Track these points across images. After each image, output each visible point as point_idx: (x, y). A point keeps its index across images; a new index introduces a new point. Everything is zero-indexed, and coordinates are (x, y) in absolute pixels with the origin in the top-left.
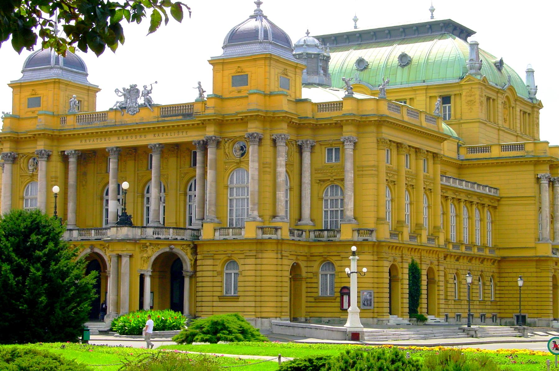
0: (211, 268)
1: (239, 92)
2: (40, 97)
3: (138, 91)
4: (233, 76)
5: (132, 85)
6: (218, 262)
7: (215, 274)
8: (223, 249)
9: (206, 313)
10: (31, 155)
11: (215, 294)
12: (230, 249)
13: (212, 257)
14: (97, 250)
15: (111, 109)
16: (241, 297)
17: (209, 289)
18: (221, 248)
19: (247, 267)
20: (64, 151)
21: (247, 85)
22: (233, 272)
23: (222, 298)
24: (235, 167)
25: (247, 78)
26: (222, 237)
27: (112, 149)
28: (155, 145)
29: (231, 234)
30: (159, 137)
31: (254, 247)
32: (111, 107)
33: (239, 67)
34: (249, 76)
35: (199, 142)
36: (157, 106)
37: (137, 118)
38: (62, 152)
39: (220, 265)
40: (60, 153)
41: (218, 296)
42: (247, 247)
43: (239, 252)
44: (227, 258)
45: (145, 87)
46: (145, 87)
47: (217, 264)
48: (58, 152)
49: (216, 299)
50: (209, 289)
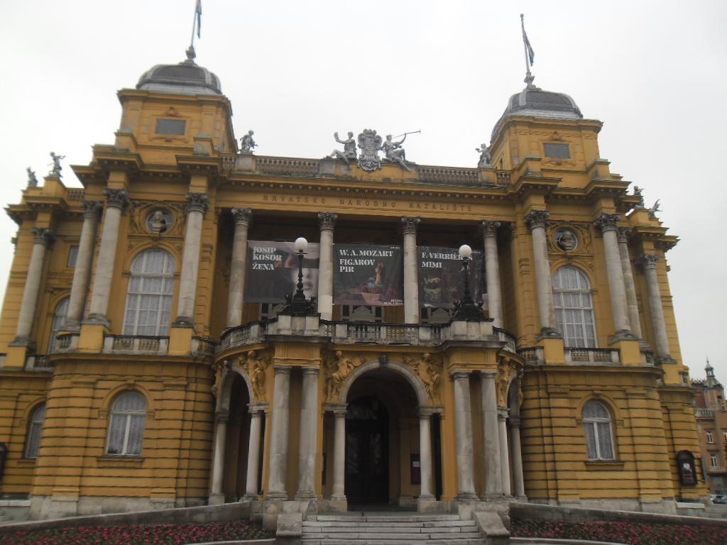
0: (566, 412)
1: (559, 164)
2: (184, 121)
3: (378, 140)
4: (544, 144)
5: (368, 129)
6: (577, 404)
7: (573, 422)
8: (583, 382)
9: (567, 492)
10: (158, 205)
11: (577, 457)
12: (596, 382)
13: (564, 395)
14: (395, 365)
15: (328, 159)
16: (627, 463)
17: (567, 448)
18: (580, 381)
19: (634, 413)
20: (231, 209)
21: (569, 158)
22: (595, 420)
23: (590, 466)
24: (565, 264)
25: (568, 149)
26: (577, 363)
27: (328, 216)
28: (412, 219)
29: (592, 358)
30: (418, 209)
31: (640, 381)
32: (329, 155)
33: (556, 133)
34: (570, 146)
35: (494, 222)
36: (413, 165)
37: (377, 176)
38: (223, 209)
39: (580, 408)
40: (220, 210)
41: (585, 462)
42: (626, 381)
43: (615, 388)
44: (591, 397)
45: (389, 138)
46: (389, 138)
47: (575, 406)
48: (217, 208)
49: (581, 466)
50: (567, 448)
